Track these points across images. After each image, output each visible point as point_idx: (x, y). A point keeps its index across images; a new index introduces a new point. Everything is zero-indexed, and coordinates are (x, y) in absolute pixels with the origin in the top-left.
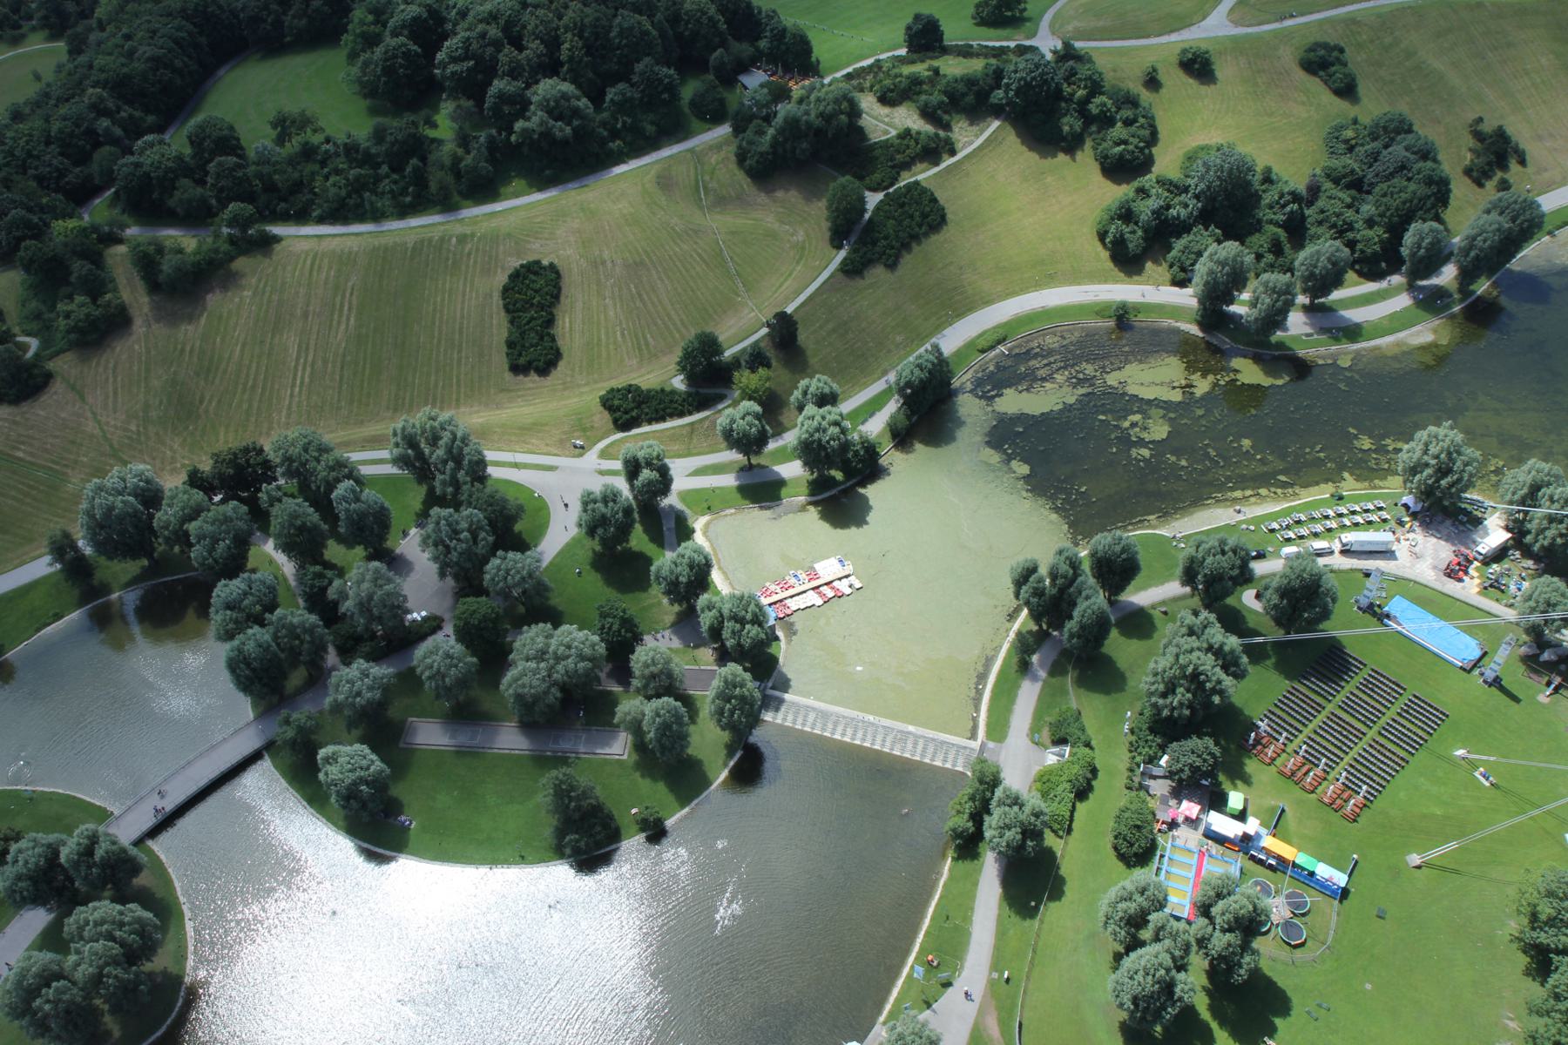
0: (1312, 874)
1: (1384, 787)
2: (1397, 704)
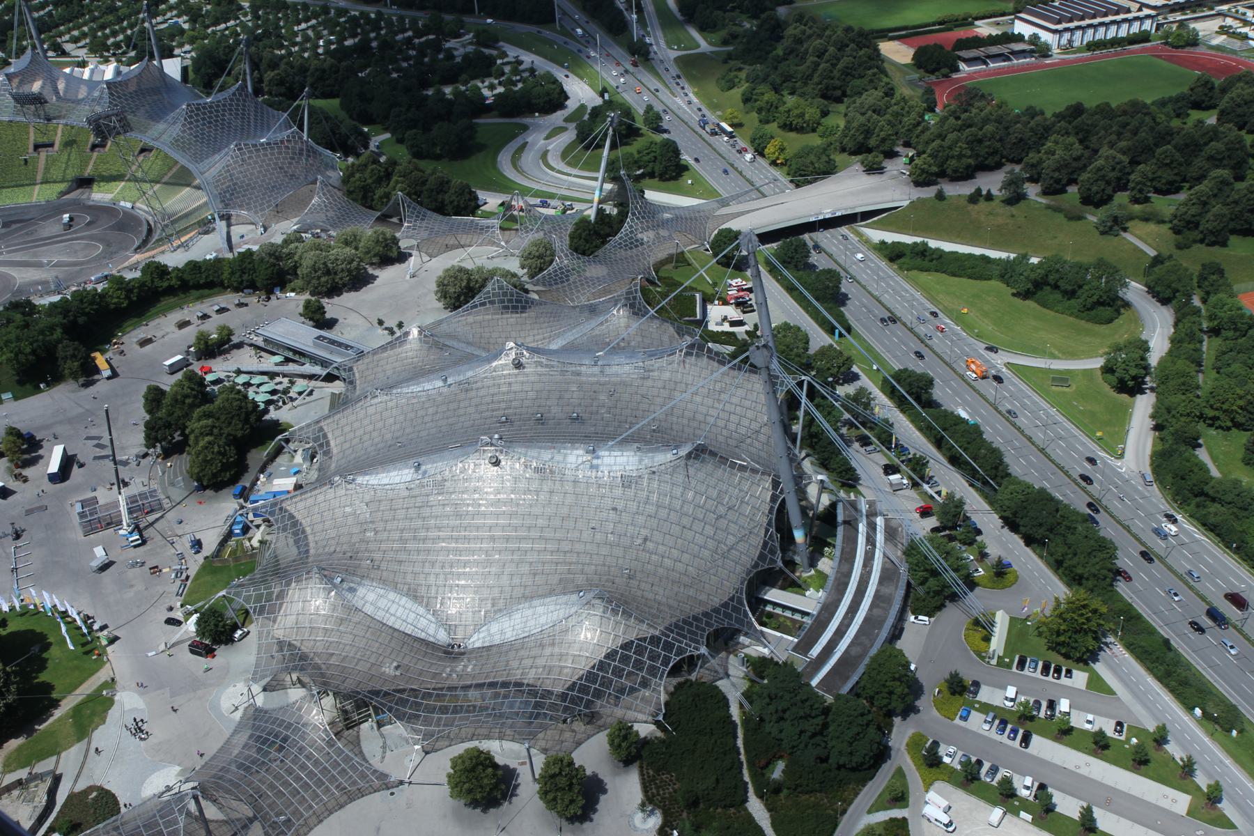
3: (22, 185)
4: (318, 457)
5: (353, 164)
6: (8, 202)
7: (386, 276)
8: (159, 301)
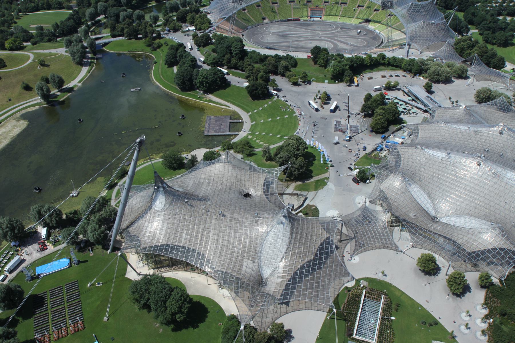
1: (82, 313)
2: (64, 292)
3: (350, 17)
4: (412, 136)
5: (461, 39)
6: (344, 21)
7: (458, 83)
8: (379, 66)
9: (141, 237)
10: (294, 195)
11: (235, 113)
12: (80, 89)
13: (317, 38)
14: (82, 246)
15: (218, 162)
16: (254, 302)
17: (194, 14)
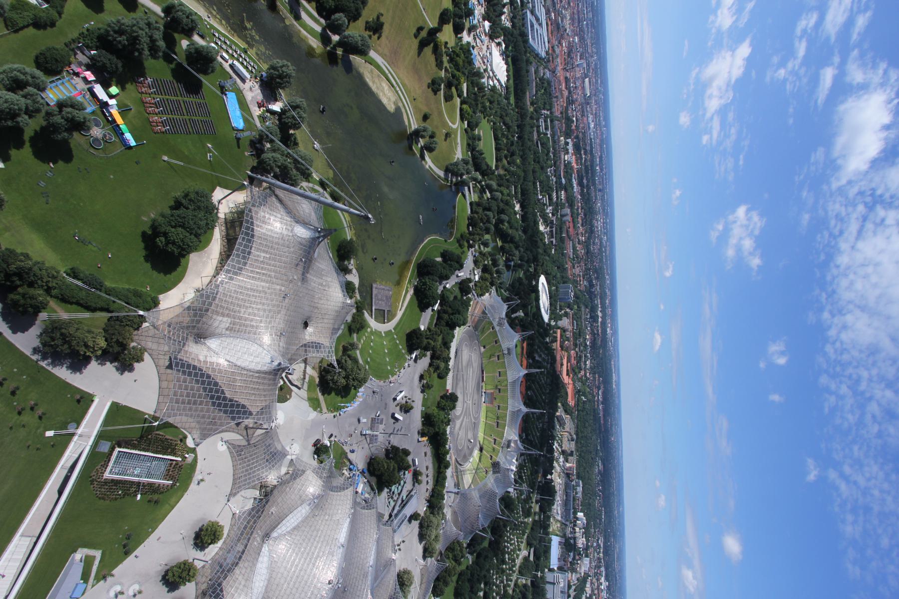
0: (123, 134)
7: (420, 548)
9: (265, 209)
10: (304, 375)
11: (394, 316)
12: (423, 167)
13: (466, 400)
14: (258, 145)
15: (344, 296)
16: (175, 328)
17: (490, 280)
